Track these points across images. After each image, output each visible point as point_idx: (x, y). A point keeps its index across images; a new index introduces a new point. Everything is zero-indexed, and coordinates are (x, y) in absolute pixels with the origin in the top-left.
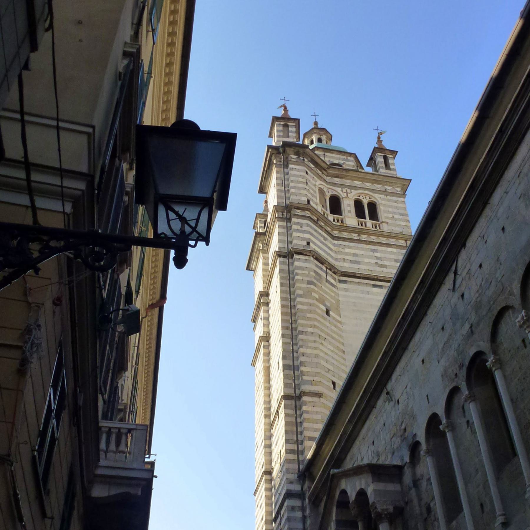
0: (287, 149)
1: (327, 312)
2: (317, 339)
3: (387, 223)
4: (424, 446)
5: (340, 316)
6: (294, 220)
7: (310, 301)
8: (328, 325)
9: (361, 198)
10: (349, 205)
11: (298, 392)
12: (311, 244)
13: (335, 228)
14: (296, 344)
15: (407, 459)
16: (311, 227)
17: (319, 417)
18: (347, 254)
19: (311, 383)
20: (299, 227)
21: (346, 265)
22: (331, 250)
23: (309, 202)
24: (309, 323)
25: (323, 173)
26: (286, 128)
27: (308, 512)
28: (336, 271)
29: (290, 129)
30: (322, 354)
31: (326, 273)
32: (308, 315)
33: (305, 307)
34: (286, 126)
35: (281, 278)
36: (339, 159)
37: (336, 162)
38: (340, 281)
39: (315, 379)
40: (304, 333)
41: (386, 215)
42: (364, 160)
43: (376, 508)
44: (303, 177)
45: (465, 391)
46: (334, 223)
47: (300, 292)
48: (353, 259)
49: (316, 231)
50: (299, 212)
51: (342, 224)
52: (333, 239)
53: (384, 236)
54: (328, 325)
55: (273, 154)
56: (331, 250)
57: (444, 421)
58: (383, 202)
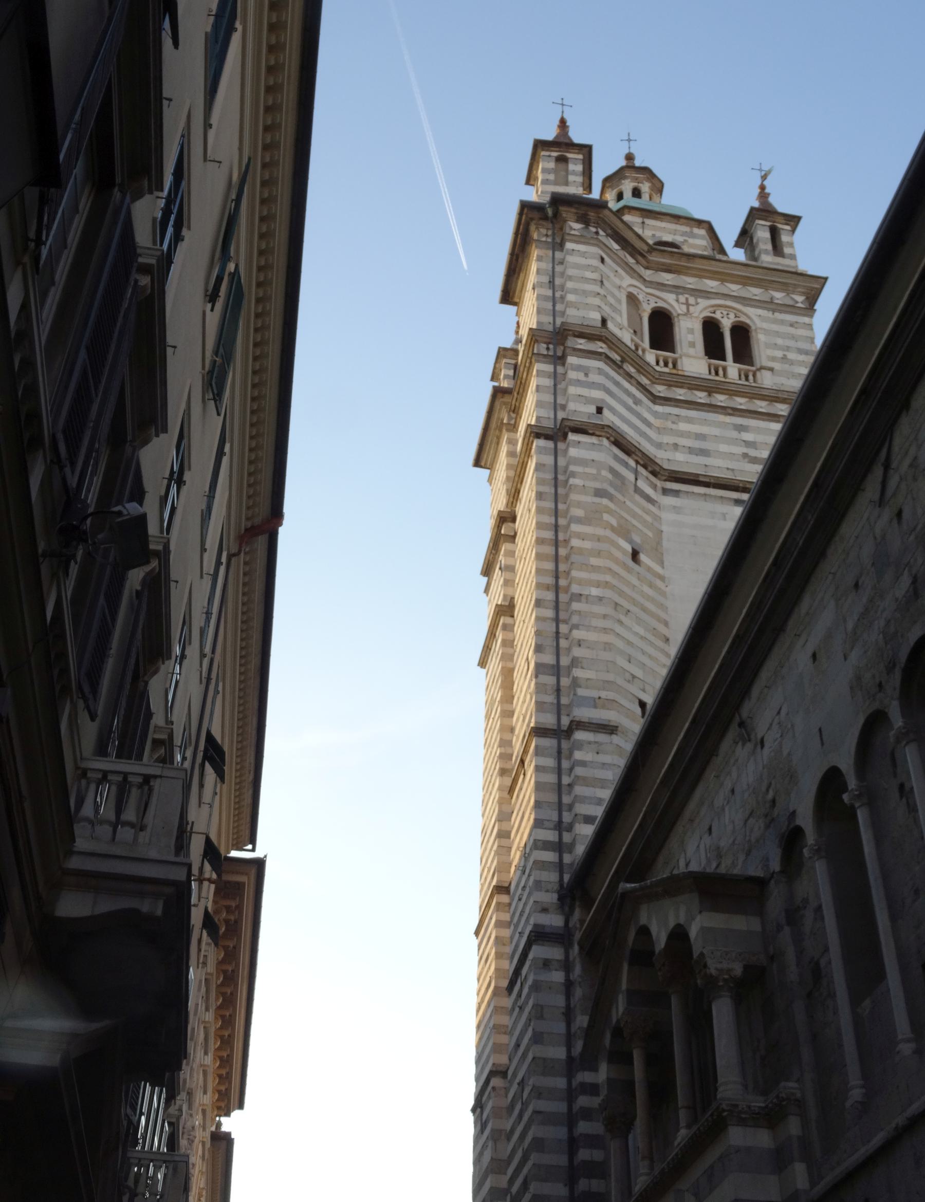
0: (562, 209)
1: (635, 555)
2: (609, 610)
3: (771, 369)
4: (810, 837)
5: (662, 563)
6: (571, 360)
7: (600, 532)
8: (635, 581)
9: (718, 316)
10: (691, 331)
11: (565, 721)
12: (606, 412)
15: (775, 865)
16: (607, 376)
18: (682, 434)
19: (595, 703)
20: (581, 376)
21: (680, 457)
23: (604, 321)
24: (595, 576)
25: (638, 262)
26: (562, 166)
27: (578, 970)
28: (657, 469)
29: (571, 167)
30: (620, 644)
31: (636, 472)
32: (594, 561)
33: (587, 545)
35: (540, 482)
36: (675, 232)
37: (668, 238)
38: (665, 492)
39: (603, 694)
40: (583, 599)
41: (770, 352)
42: (728, 235)
43: (705, 966)
44: (595, 269)
45: (897, 721)
46: (658, 368)
47: (578, 512)
48: (697, 444)
49: (617, 384)
50: (582, 344)
51: (674, 371)
52: (654, 403)
53: (763, 398)
54: (635, 581)
55: (532, 219)
57: (852, 783)
58: (765, 325)
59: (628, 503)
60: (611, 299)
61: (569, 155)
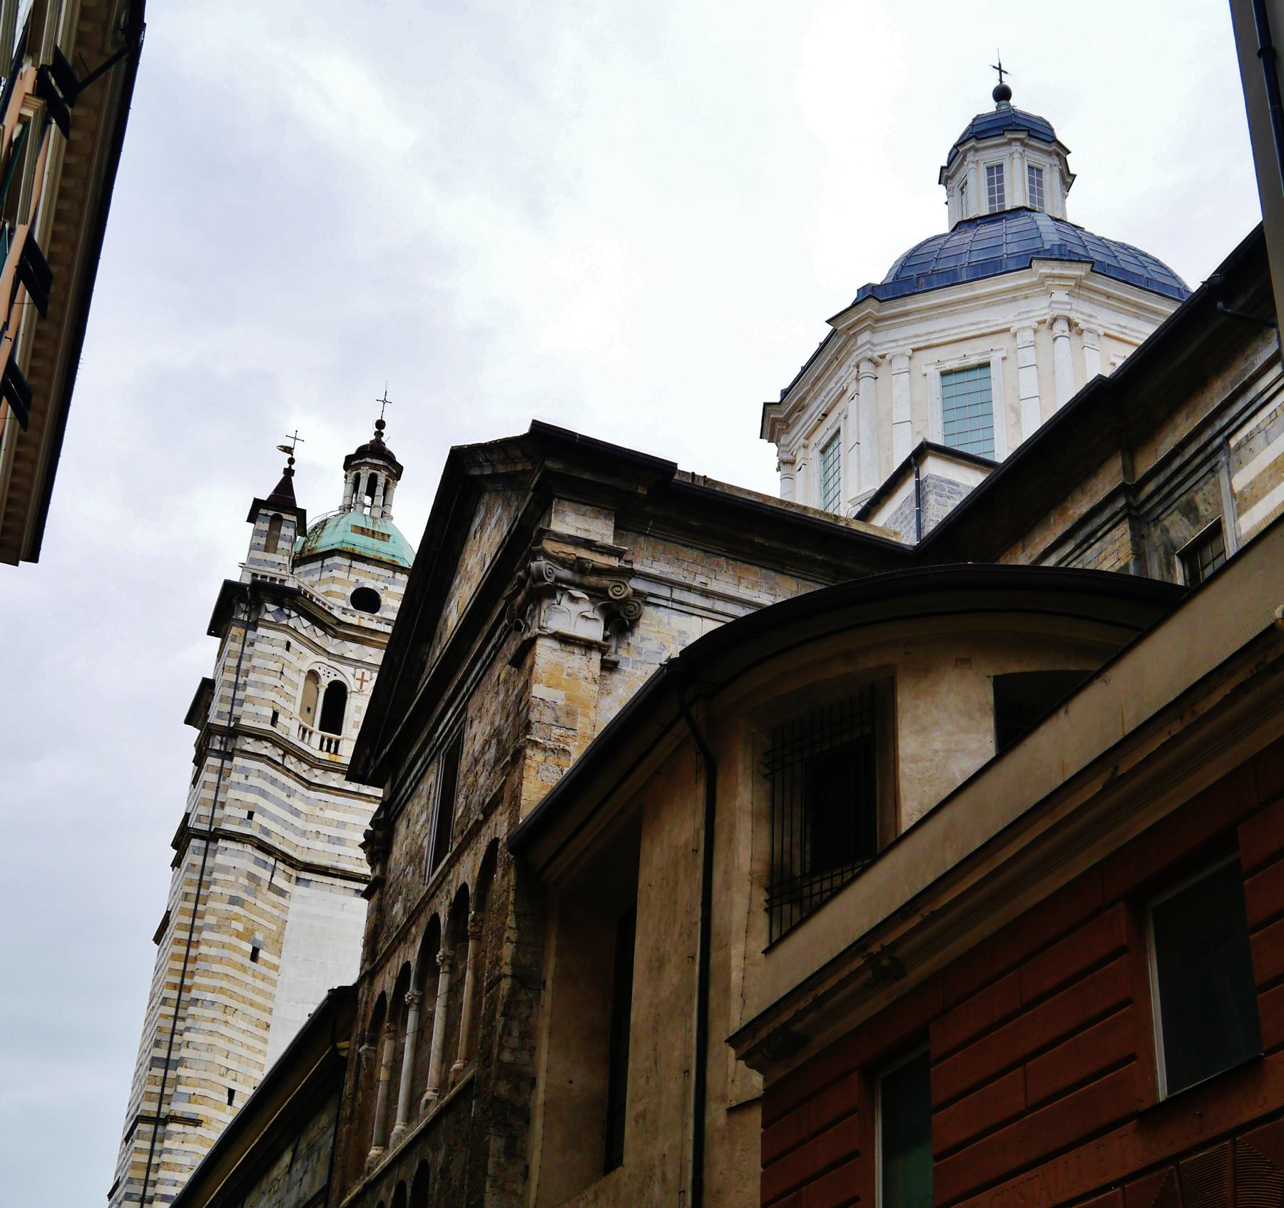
1: (254, 956)
11: (165, 1109)
12: (256, 816)
13: (314, 763)
14: (183, 1019)
17: (187, 1161)
19: (191, 1098)
22: (296, 813)
23: (275, 715)
30: (221, 1043)
32: (216, 968)
33: (213, 951)
34: (276, 522)
37: (369, 584)
39: (198, 1091)
40: (199, 1004)
49: (274, 781)
50: (250, 745)
51: (333, 758)
52: (308, 789)
56: (296, 813)
59: (259, 904)
60: (288, 689)
61: (285, 516)
